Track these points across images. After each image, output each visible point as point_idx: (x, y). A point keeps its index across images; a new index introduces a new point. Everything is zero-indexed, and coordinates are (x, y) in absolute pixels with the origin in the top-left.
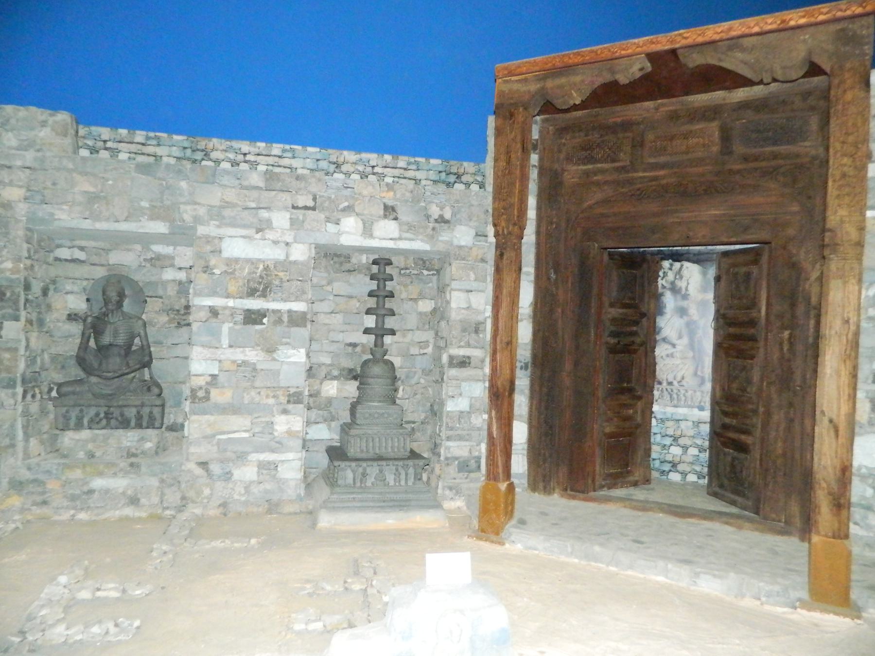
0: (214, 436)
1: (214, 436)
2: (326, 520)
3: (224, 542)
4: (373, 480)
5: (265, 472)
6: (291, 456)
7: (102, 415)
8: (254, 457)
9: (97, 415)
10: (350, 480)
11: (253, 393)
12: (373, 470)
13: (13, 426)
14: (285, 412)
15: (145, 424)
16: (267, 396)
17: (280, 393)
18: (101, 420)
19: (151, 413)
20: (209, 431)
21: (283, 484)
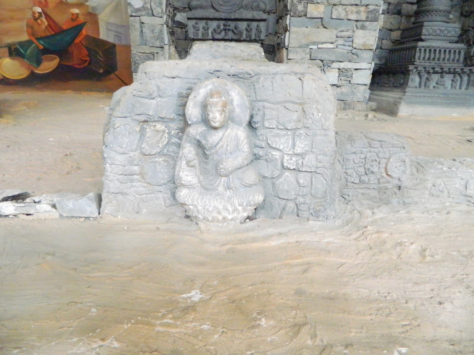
0: (308, 45)
1: (308, 45)
2: (404, 110)
3: (347, 115)
4: (434, 84)
5: (342, 78)
6: (364, 65)
7: (222, 27)
8: (335, 65)
9: (218, 27)
10: (417, 84)
11: (340, 8)
12: (436, 77)
13: (161, 31)
14: (363, 28)
15: (253, 37)
16: (352, 13)
17: (362, 9)
18: (221, 31)
19: (258, 26)
20: (304, 42)
21: (355, 89)
